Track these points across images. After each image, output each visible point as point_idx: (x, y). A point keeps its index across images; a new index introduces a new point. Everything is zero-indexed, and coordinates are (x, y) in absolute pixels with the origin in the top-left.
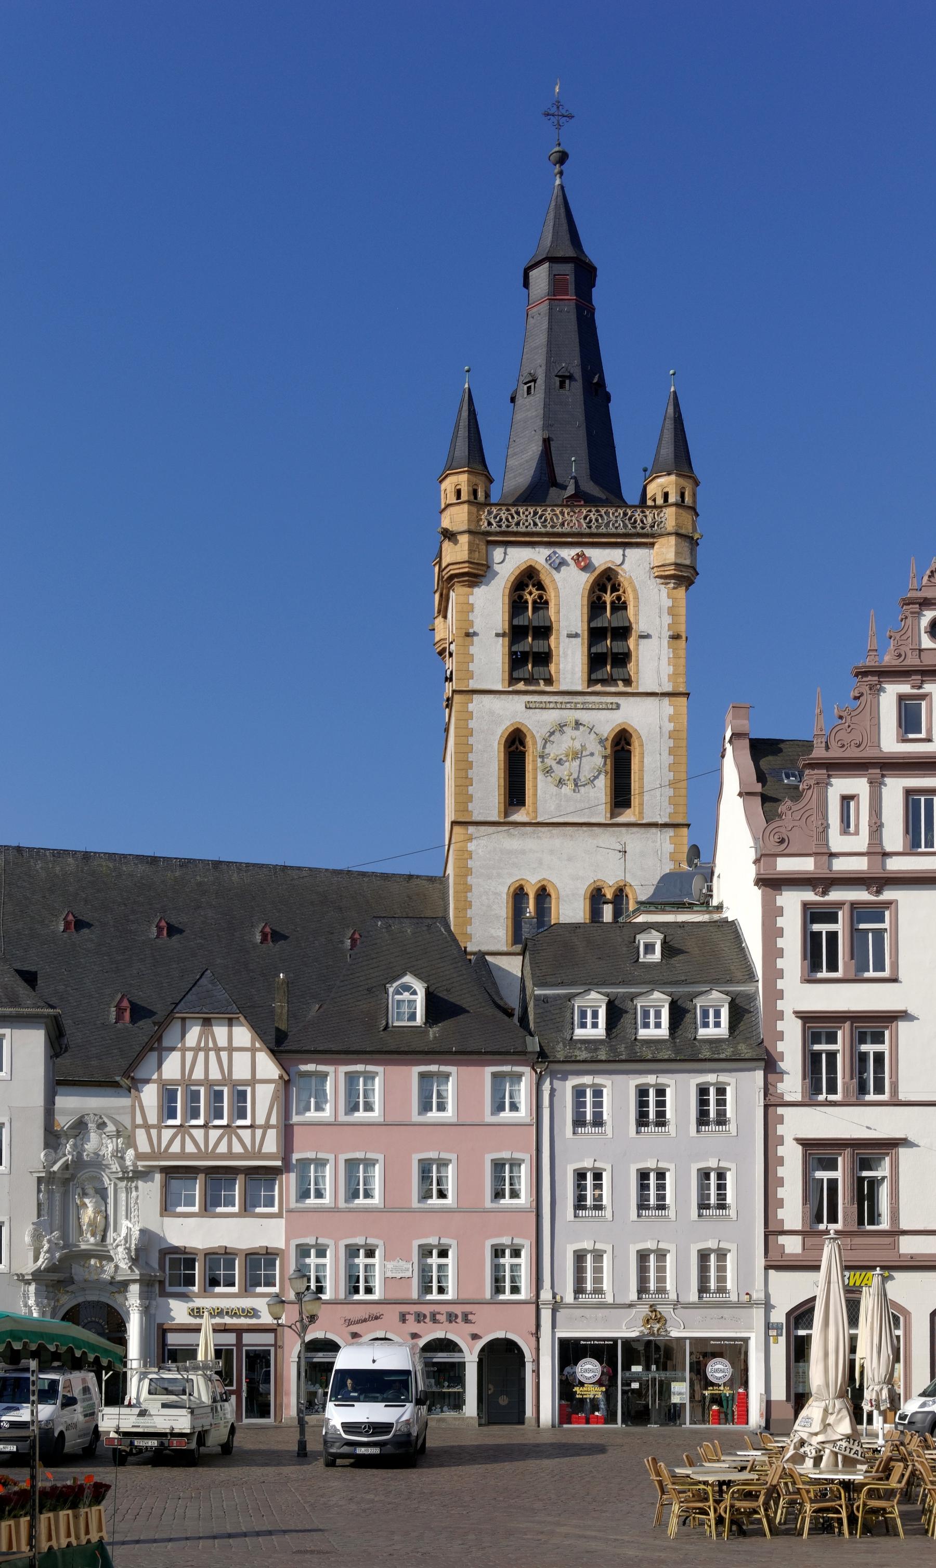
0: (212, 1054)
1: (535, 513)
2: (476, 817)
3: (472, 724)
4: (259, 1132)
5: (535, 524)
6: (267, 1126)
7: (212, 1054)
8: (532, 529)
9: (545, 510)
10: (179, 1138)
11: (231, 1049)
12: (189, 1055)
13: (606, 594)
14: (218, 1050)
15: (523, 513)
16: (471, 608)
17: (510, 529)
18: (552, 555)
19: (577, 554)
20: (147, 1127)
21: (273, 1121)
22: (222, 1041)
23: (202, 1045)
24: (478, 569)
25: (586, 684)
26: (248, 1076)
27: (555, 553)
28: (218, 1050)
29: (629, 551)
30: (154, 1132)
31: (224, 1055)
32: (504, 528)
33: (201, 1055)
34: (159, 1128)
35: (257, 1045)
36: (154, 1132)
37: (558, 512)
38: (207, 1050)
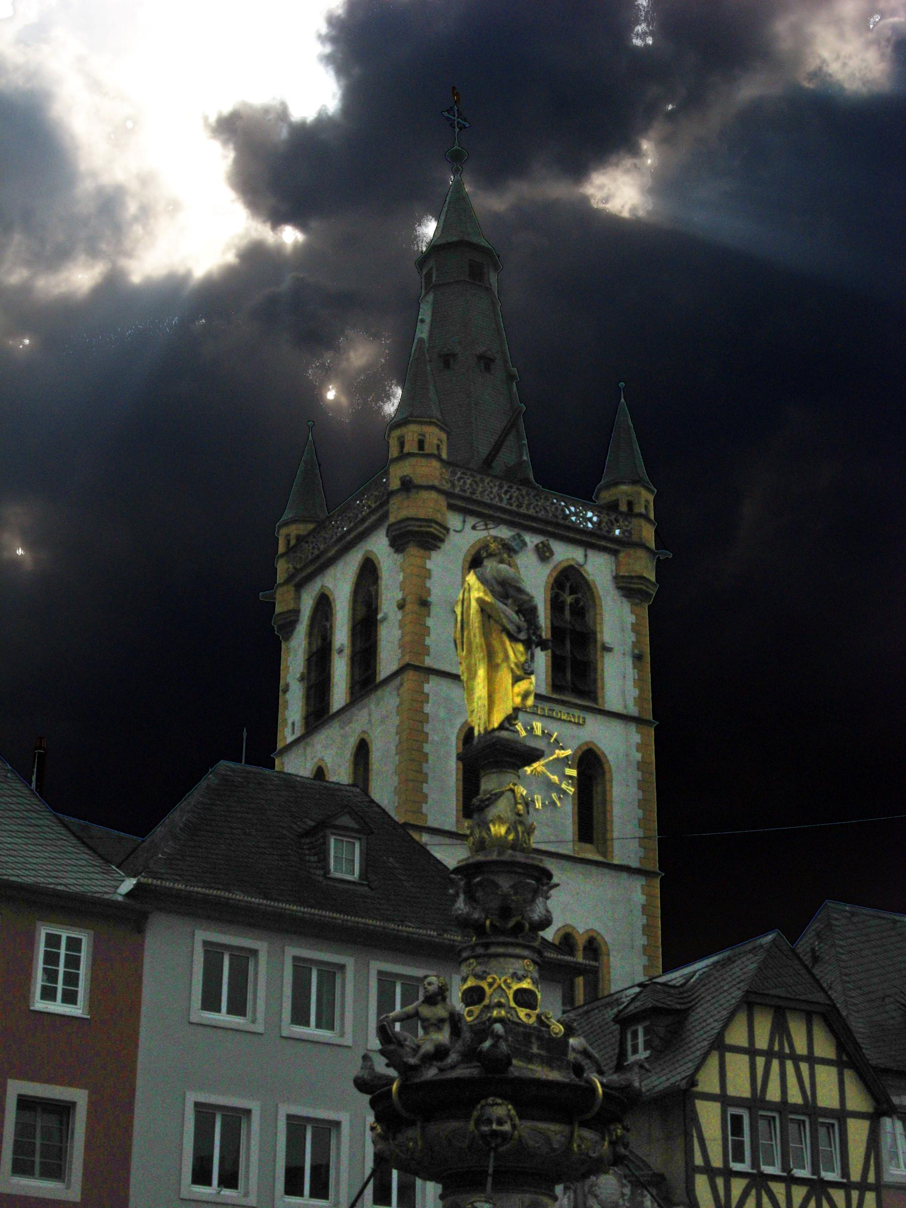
0: (789, 1065)
1: (501, 487)
2: (432, 823)
3: (428, 709)
4: (855, 1194)
5: (501, 499)
6: (863, 1187)
7: (789, 1065)
8: (496, 501)
9: (511, 487)
10: (753, 1192)
11: (812, 1060)
12: (760, 1061)
13: (564, 593)
14: (796, 1059)
15: (488, 483)
16: (428, 574)
17: (474, 497)
18: (516, 537)
19: (542, 543)
20: (710, 1172)
21: (871, 1179)
22: (801, 1048)
23: (776, 1048)
24: (438, 531)
25: (550, 689)
26: (835, 1104)
27: (519, 535)
28: (796, 1059)
29: (590, 553)
30: (720, 1182)
31: (804, 1067)
32: (468, 494)
33: (775, 1064)
34: (728, 1174)
35: (845, 1058)
36: (720, 1182)
37: (524, 492)
38: (782, 1058)
